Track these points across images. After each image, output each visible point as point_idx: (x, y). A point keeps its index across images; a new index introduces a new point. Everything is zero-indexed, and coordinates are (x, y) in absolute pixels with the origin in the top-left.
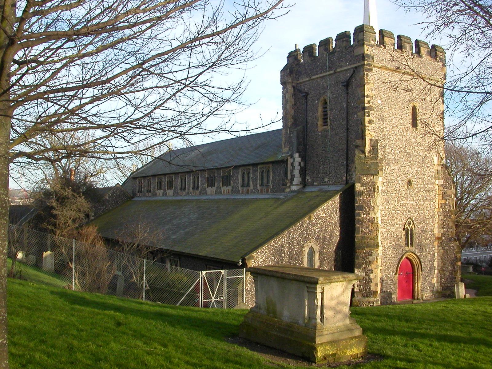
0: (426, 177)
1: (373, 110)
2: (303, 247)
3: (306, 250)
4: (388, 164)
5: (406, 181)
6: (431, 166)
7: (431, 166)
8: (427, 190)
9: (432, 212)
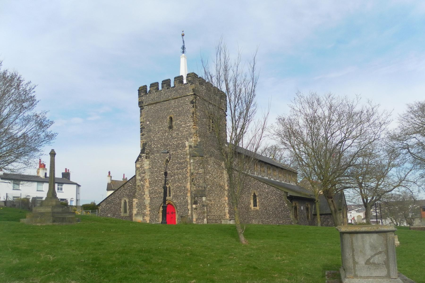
0: (179, 156)
1: (145, 128)
2: (121, 200)
3: (123, 202)
4: (153, 154)
5: (165, 160)
6: (183, 148)
7: (183, 148)
8: (180, 163)
9: (184, 175)
